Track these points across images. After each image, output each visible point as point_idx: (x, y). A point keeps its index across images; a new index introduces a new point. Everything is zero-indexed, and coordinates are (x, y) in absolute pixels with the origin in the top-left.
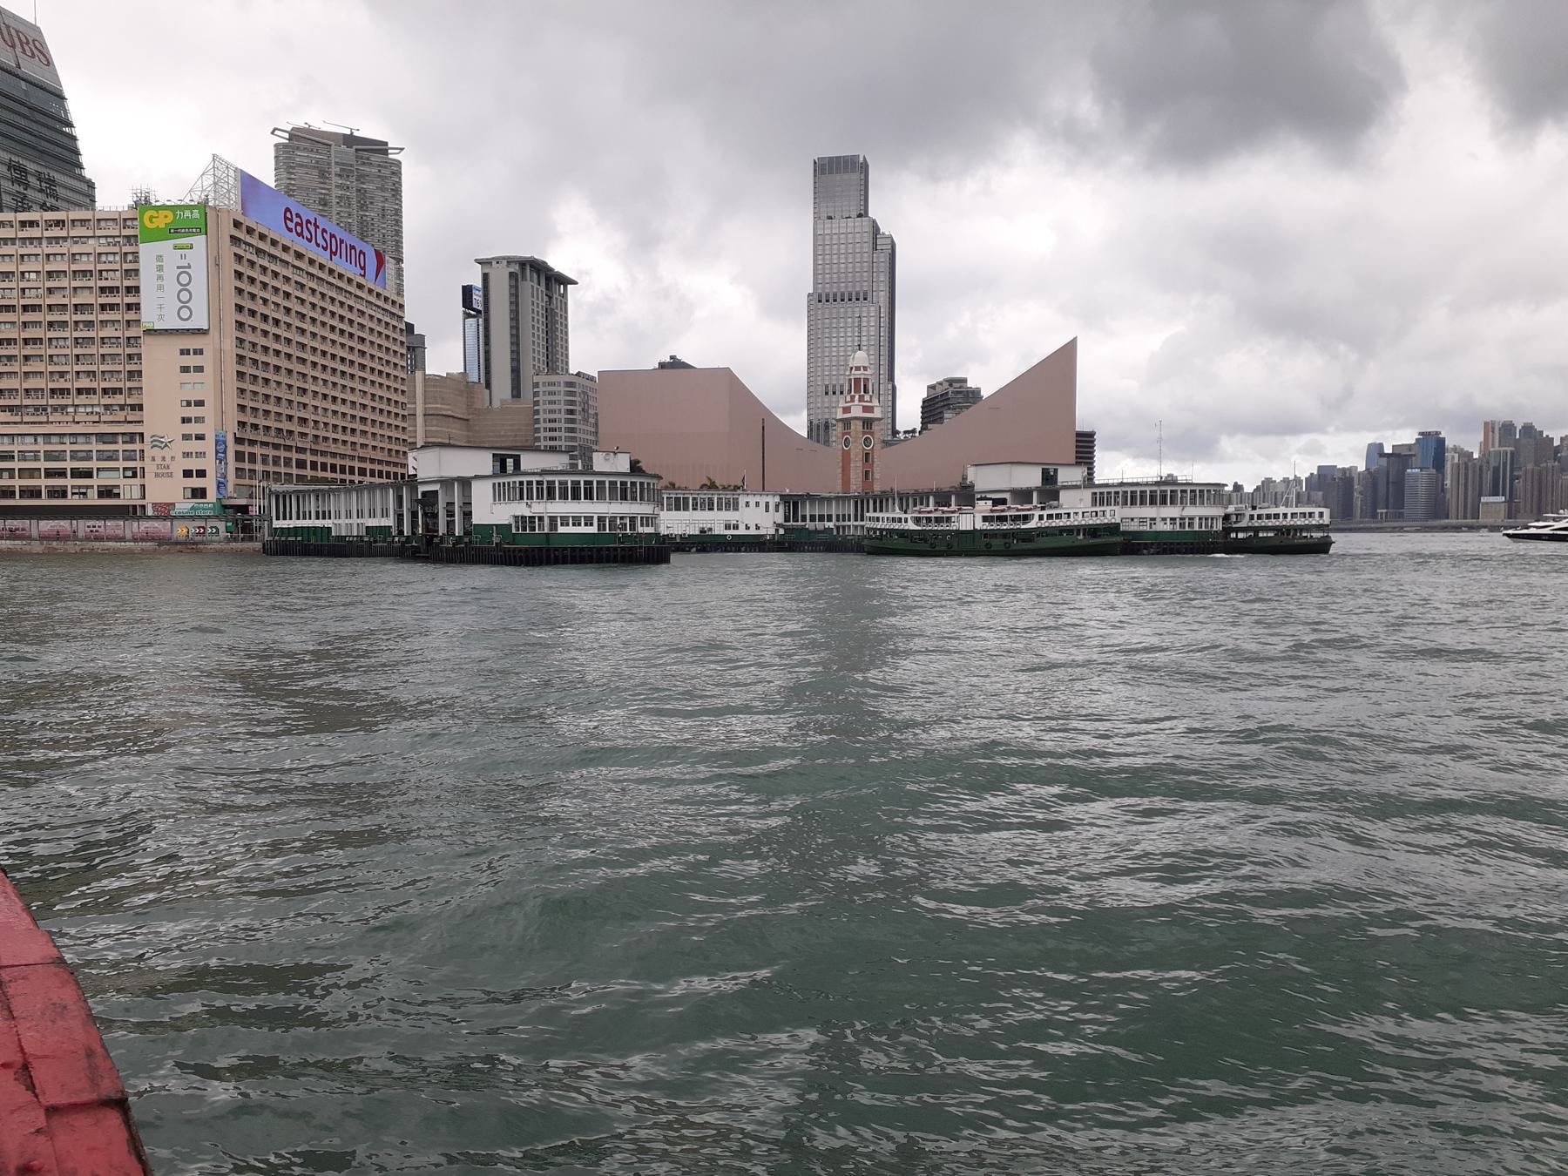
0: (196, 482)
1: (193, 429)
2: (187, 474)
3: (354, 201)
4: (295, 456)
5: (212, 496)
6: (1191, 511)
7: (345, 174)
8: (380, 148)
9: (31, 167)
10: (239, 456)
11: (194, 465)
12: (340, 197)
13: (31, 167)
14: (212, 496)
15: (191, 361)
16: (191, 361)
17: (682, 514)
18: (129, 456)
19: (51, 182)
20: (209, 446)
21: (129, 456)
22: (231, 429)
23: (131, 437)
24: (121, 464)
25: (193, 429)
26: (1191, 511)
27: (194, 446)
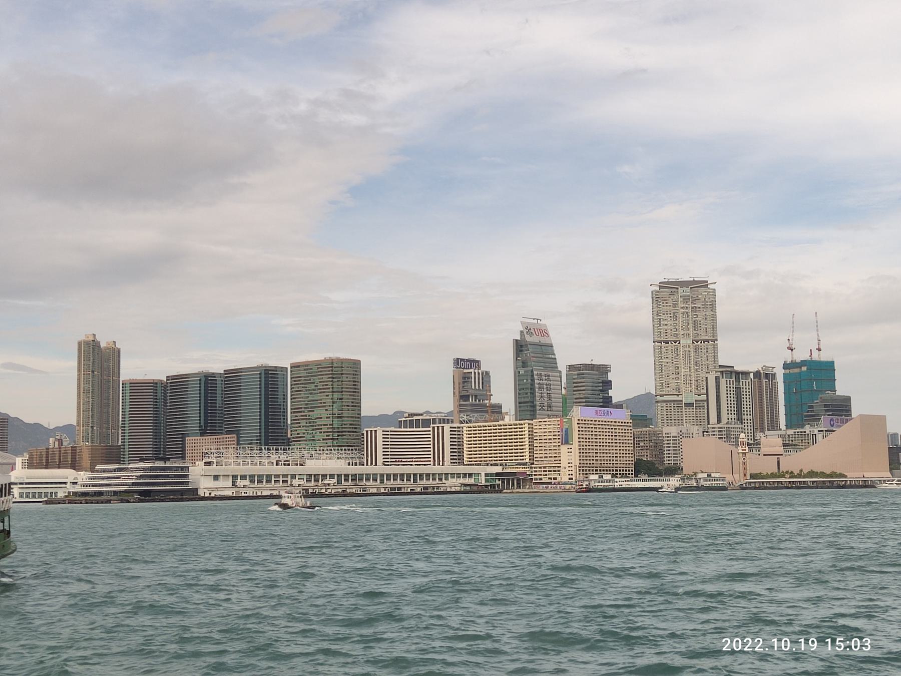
0: (571, 476)
1: (570, 465)
2: (569, 475)
3: (690, 314)
4: (594, 469)
5: (574, 480)
6: (712, 482)
7: (685, 301)
8: (704, 284)
9: (543, 373)
10: (579, 470)
11: (570, 473)
12: (683, 313)
13: (543, 373)
14: (574, 480)
15: (570, 450)
16: (570, 450)
17: (657, 482)
18: (559, 471)
19: (549, 376)
20: (573, 469)
21: (559, 471)
22: (578, 465)
23: (559, 467)
24: (557, 473)
25: (570, 465)
26: (712, 482)
27: (570, 469)
